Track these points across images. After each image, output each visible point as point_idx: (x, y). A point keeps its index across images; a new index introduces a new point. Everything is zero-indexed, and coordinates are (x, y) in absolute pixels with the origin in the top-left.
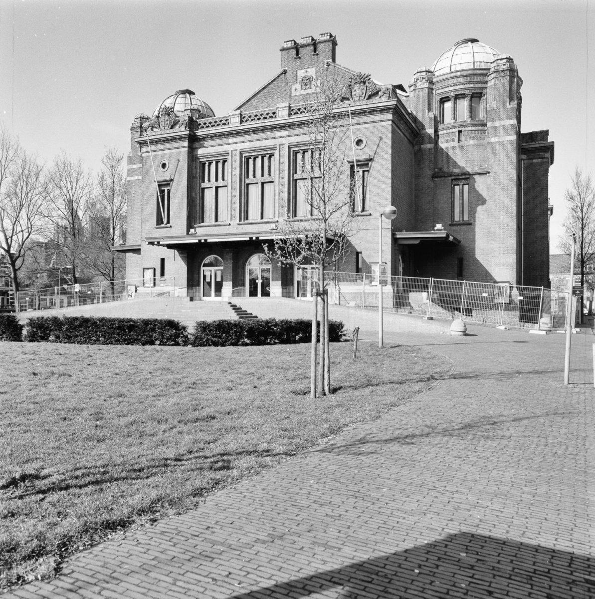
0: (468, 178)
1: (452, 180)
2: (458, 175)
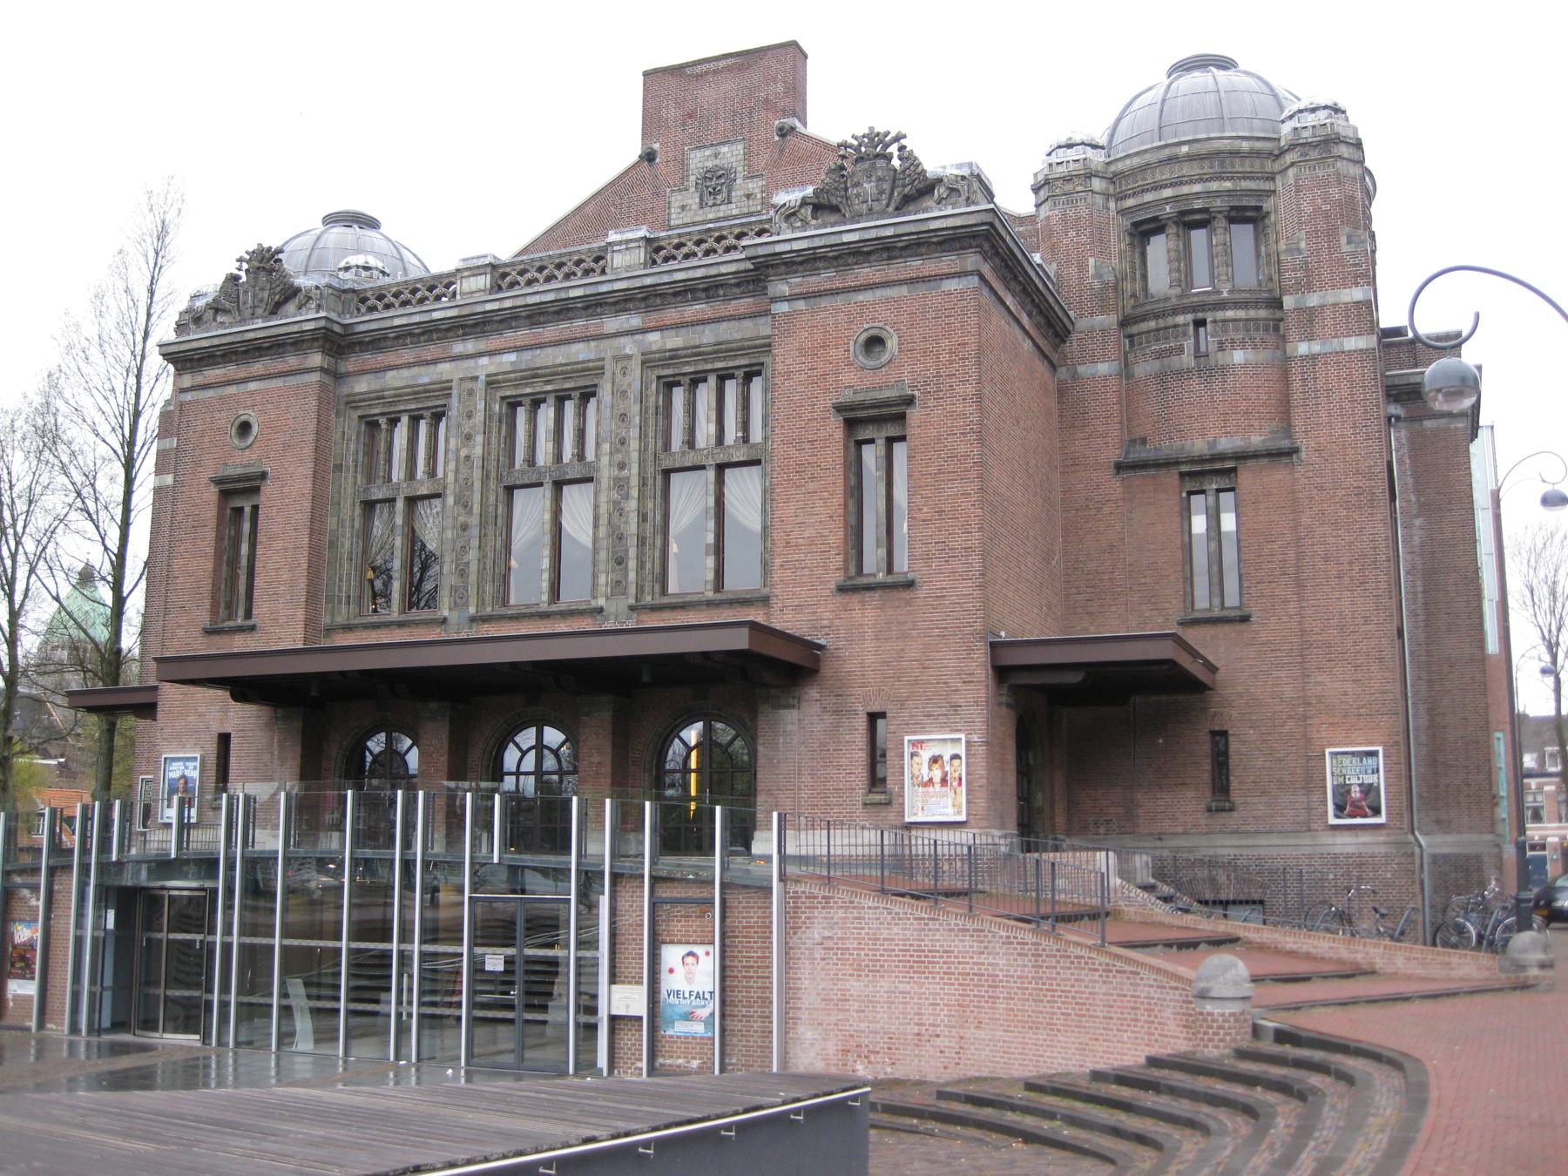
0: (1234, 470)
1: (1182, 475)
2: (1201, 460)
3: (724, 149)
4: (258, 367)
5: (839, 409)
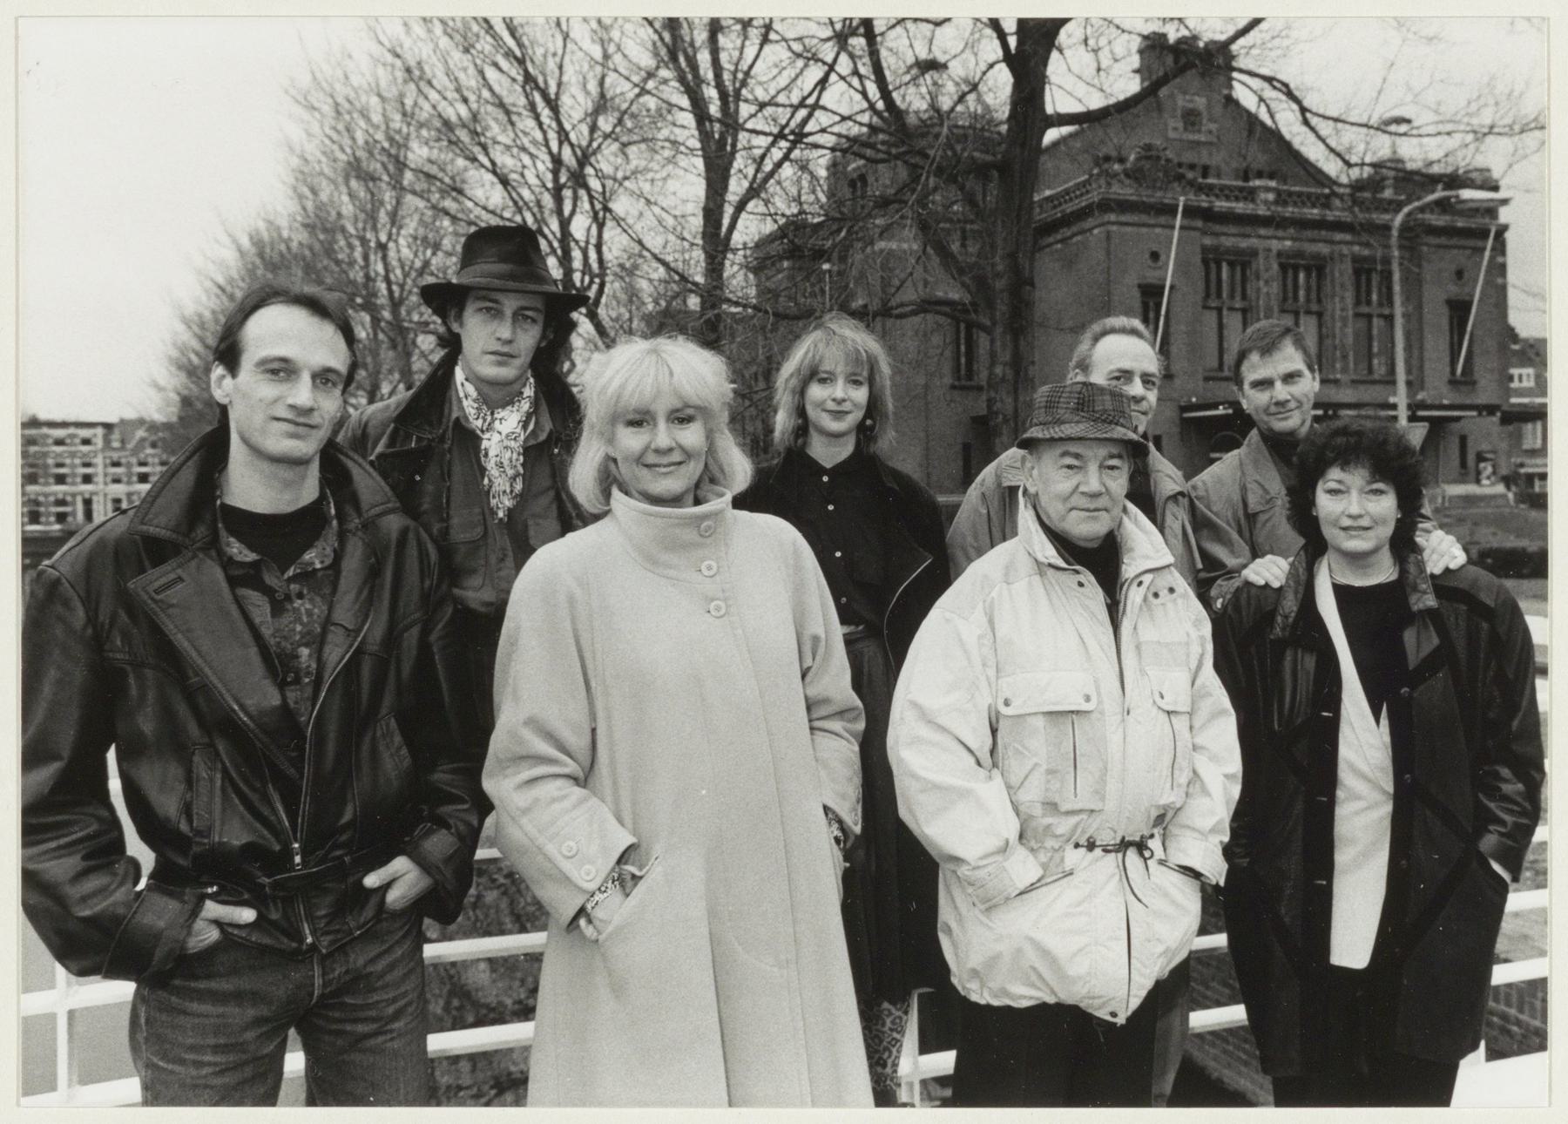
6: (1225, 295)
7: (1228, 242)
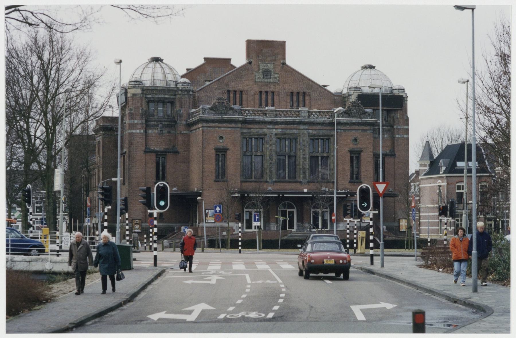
3: (269, 65)
4: (225, 125)
5: (349, 151)
6: (253, 150)
7: (254, 131)
